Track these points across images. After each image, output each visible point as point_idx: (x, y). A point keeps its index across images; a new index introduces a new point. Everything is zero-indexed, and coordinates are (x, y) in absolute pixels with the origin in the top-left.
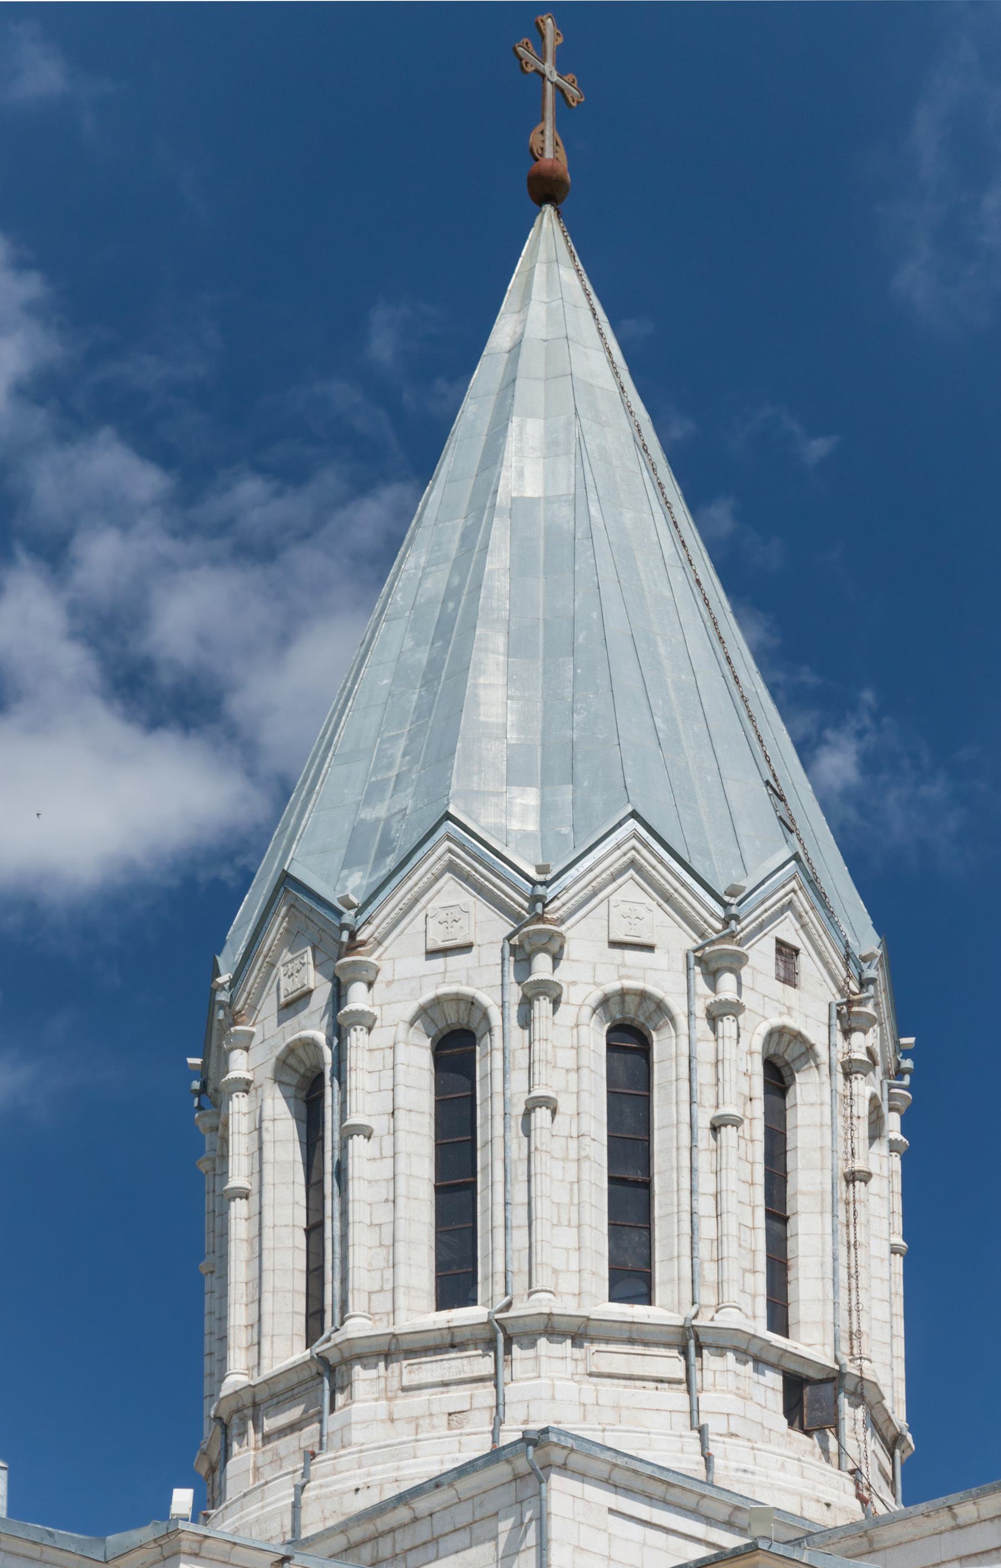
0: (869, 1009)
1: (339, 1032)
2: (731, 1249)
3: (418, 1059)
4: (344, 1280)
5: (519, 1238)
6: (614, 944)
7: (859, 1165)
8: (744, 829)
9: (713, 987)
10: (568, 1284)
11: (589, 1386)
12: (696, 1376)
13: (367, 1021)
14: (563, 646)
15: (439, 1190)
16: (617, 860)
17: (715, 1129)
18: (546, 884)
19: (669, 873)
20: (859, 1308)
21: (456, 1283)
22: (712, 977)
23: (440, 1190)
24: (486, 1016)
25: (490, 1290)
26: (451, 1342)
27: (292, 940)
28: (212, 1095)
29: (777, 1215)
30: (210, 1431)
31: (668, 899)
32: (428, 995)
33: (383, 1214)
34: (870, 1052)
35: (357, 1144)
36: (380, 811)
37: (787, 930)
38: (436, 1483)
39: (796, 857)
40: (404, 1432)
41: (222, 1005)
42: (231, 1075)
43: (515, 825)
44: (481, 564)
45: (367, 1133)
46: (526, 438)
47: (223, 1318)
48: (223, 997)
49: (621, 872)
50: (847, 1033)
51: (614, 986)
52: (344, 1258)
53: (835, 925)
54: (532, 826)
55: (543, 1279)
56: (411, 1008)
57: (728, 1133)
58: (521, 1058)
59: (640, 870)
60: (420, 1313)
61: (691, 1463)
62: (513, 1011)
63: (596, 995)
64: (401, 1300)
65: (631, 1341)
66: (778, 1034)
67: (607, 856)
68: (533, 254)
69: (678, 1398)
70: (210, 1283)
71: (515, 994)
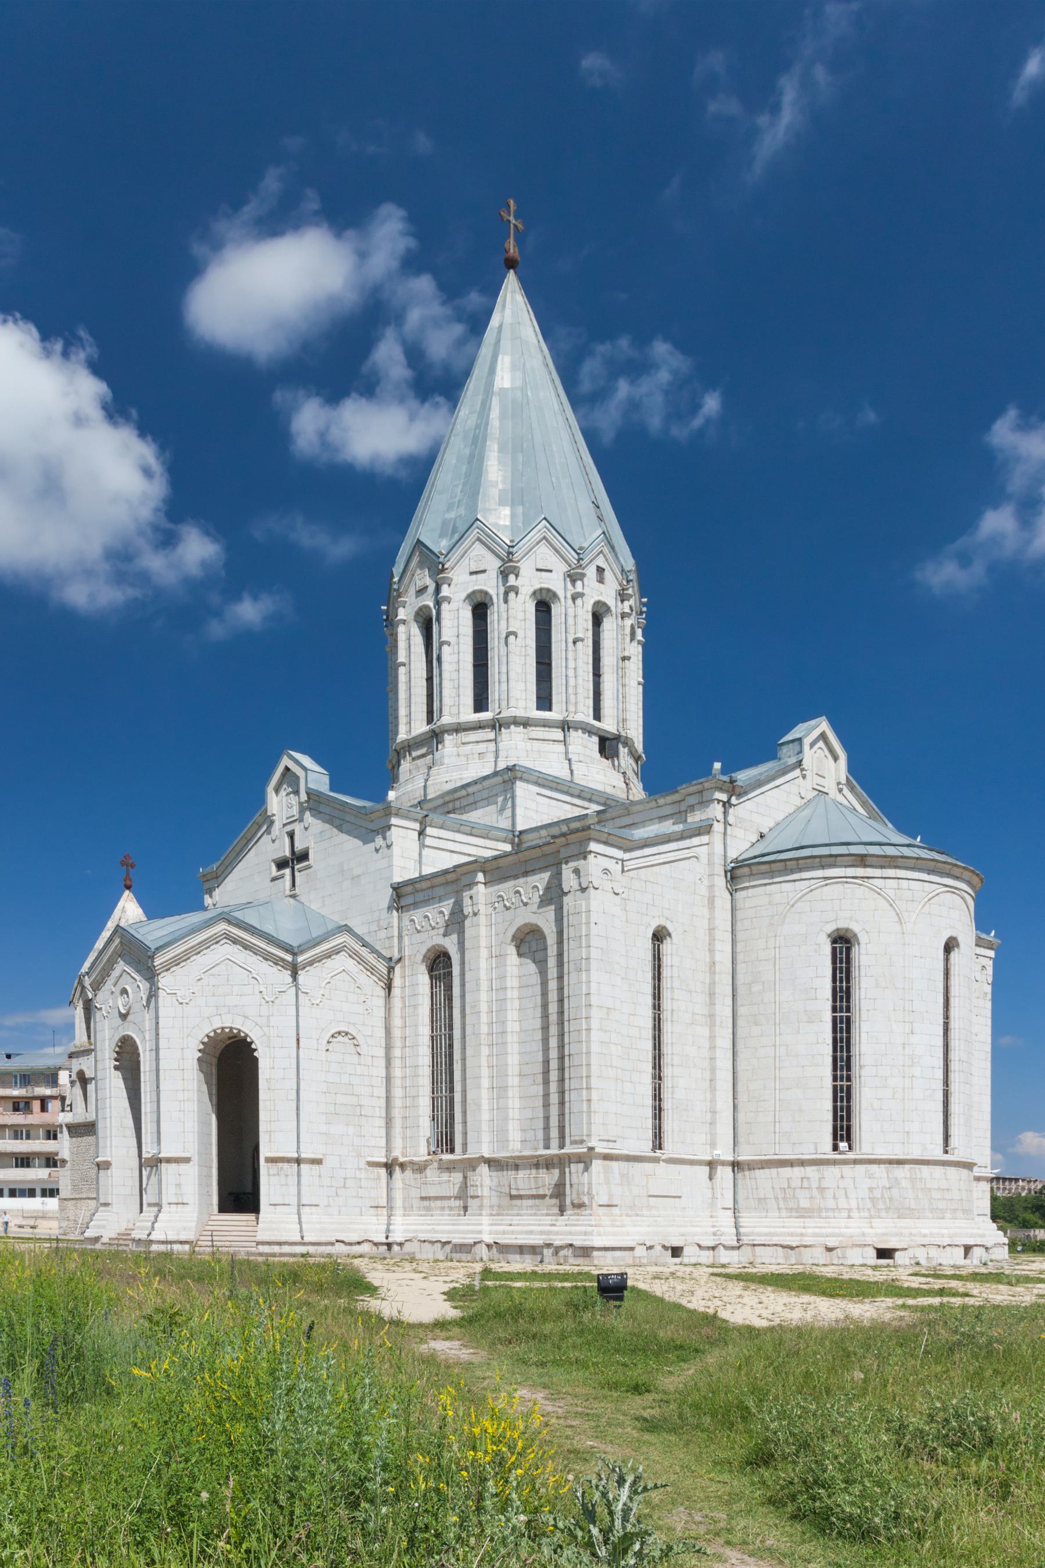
0: (630, 591)
1: (438, 603)
2: (580, 690)
3: (467, 614)
4: (441, 701)
5: (504, 686)
6: (538, 570)
7: (626, 654)
9: (574, 586)
10: (521, 704)
12: (568, 739)
13: (448, 600)
14: (518, 448)
15: (475, 666)
16: (538, 537)
17: (574, 643)
18: (513, 547)
19: (558, 542)
20: (626, 711)
21: (481, 703)
24: (491, 599)
26: (479, 726)
27: (421, 565)
28: (391, 622)
29: (597, 674)
30: (392, 755)
31: (557, 551)
32: (470, 590)
33: (455, 676)
34: (631, 607)
35: (445, 648)
36: (452, 515)
37: (601, 562)
38: (475, 782)
39: (604, 533)
41: (395, 590)
42: (399, 618)
43: (502, 522)
44: (488, 415)
45: (448, 644)
46: (504, 362)
47: (396, 710)
48: (395, 587)
49: (540, 541)
50: (622, 601)
51: (538, 586)
52: (441, 692)
54: (508, 523)
55: (512, 703)
56: (464, 595)
57: (579, 644)
58: (504, 615)
59: (547, 540)
60: (469, 716)
62: (501, 597)
63: (531, 590)
64: (462, 709)
65: (544, 726)
66: (597, 603)
67: (535, 535)
68: (507, 287)
70: (390, 695)
71: (502, 590)
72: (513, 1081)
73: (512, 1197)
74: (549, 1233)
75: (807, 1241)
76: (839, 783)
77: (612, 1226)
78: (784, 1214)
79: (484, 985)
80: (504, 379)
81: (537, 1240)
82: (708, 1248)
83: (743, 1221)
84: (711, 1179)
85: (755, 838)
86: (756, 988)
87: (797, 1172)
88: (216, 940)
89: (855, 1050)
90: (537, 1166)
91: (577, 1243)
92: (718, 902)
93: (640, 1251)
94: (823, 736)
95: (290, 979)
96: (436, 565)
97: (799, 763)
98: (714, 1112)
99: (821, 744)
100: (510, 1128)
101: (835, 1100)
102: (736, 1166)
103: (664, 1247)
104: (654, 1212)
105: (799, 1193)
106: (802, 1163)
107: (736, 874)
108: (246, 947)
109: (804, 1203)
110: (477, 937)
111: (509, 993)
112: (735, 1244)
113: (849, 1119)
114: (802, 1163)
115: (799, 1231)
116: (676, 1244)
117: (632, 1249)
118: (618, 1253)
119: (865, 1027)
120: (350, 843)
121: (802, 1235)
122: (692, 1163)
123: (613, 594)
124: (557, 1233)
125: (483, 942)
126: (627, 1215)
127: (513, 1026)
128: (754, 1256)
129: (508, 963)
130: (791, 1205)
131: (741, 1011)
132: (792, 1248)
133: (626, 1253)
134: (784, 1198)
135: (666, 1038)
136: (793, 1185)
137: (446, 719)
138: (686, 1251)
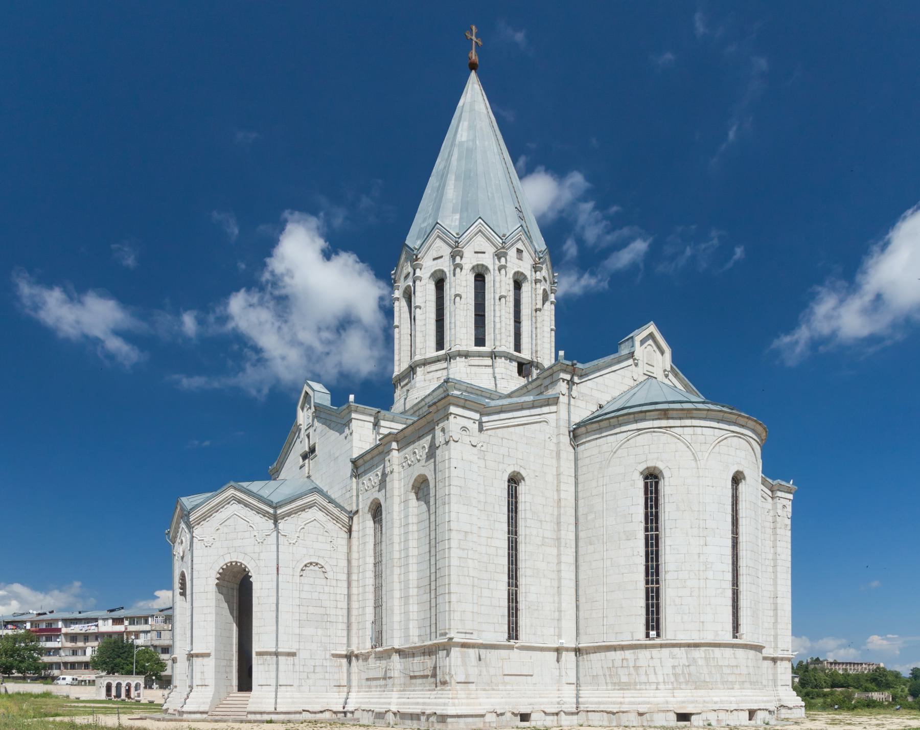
1: (414, 282)
3: (432, 287)
6: (476, 252)
8: (509, 219)
13: (420, 279)
22: (499, 259)
27: (406, 260)
37: (520, 245)
45: (420, 307)
51: (475, 263)
53: (531, 242)
56: (429, 274)
63: (471, 266)
71: (452, 268)
72: (413, 592)
75: (624, 708)
76: (665, 371)
77: (467, 698)
78: (610, 687)
79: (397, 523)
81: (417, 710)
82: (553, 714)
84: (558, 661)
85: (594, 408)
87: (619, 655)
88: (227, 502)
89: (662, 560)
90: (424, 654)
91: (438, 712)
92: (563, 455)
94: (651, 336)
95: (273, 526)
96: (414, 259)
97: (631, 355)
98: (560, 611)
99: (650, 342)
100: (411, 626)
101: (647, 599)
102: (578, 651)
103: (514, 714)
104: (509, 687)
105: (622, 672)
106: (622, 648)
107: (577, 434)
108: (246, 505)
109: (624, 679)
110: (392, 489)
111: (411, 528)
112: (574, 710)
113: (658, 613)
114: (622, 648)
117: (483, 716)
118: (470, 720)
119: (668, 542)
120: (333, 434)
121: (621, 703)
122: (542, 649)
123: (529, 267)
124: (429, 704)
125: (396, 492)
126: (485, 690)
127: (413, 552)
128: (588, 720)
129: (410, 505)
130: (615, 680)
131: (582, 535)
132: (614, 714)
133: (477, 719)
135: (522, 556)
136: (616, 665)
138: (533, 717)
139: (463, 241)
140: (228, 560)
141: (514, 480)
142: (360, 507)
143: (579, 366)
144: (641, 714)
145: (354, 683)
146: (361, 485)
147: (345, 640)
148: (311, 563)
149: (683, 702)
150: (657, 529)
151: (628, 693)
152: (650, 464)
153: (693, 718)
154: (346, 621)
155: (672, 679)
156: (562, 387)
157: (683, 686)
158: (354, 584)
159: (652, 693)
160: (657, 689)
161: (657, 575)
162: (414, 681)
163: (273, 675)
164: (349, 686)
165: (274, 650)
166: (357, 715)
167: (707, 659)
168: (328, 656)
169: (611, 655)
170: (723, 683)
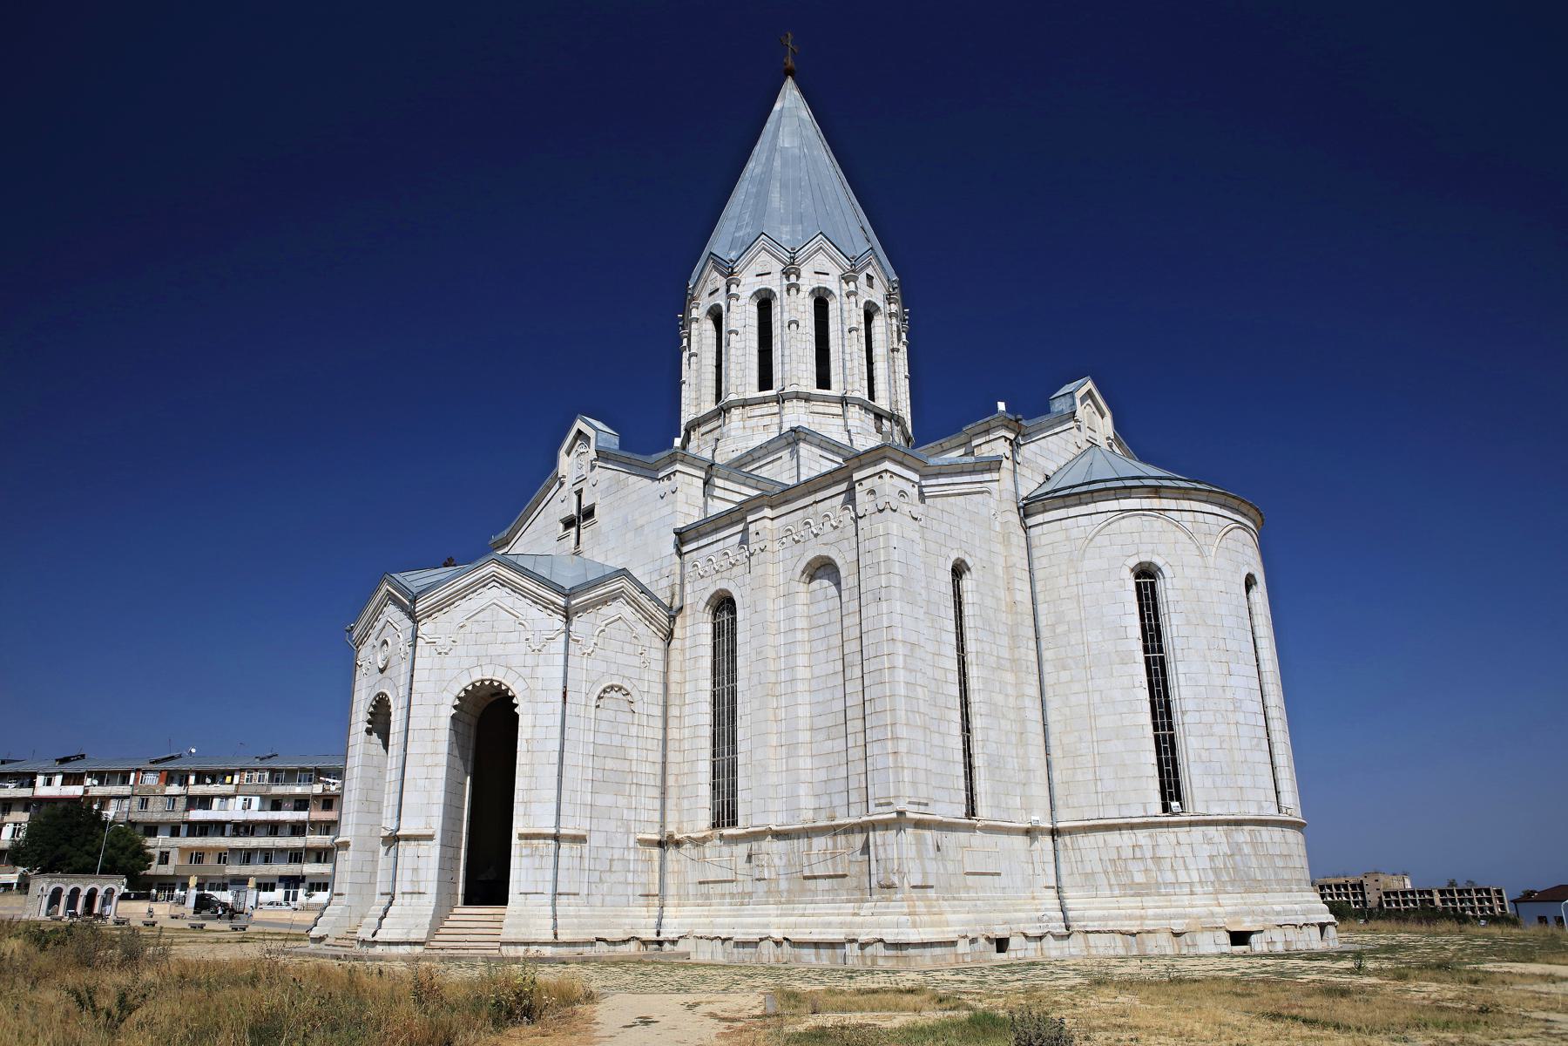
3: (753, 310)
11: (811, 417)
19: (833, 251)
20: (895, 392)
21: (765, 381)
23: (760, 352)
25: (777, 385)
28: (687, 322)
37: (870, 271)
38: (761, 447)
40: (749, 432)
60: (753, 392)
61: (845, 441)
66: (868, 303)
67: (813, 246)
69: (840, 421)
73: (806, 878)
74: (851, 925)
75: (1150, 925)
77: (929, 913)
78: (1117, 892)
80: (786, 141)
83: (1069, 903)
86: (1060, 629)
87: (1127, 838)
91: (889, 938)
92: (1014, 539)
93: (963, 946)
97: (1073, 415)
102: (1054, 833)
103: (988, 939)
105: (1134, 867)
106: (1132, 827)
109: (1140, 878)
115: (1138, 912)
116: (1000, 933)
117: (953, 943)
118: (938, 951)
121: (1142, 917)
122: (1009, 831)
124: (862, 926)
128: (1088, 947)
130: (1124, 880)
131: (1046, 655)
132: (1133, 935)
134: (1115, 872)
137: (732, 397)
138: (1013, 943)
139: (801, 256)
140: (477, 676)
141: (958, 571)
142: (688, 600)
143: (1024, 422)
144: (1177, 935)
145: (671, 889)
146: (689, 568)
147: (657, 816)
148: (612, 687)
149: (1235, 913)
150: (1161, 650)
151: (1149, 901)
152: (1145, 558)
153: (1253, 938)
154: (659, 783)
155: (1212, 878)
156: (1002, 448)
157: (1229, 888)
158: (672, 723)
159: (1186, 900)
160: (1192, 893)
161: (1169, 716)
162: (811, 884)
163: (549, 875)
164: (662, 895)
165: (553, 831)
166: (681, 947)
167: (1253, 844)
168: (632, 844)
169: (1113, 838)
170: (1278, 881)
